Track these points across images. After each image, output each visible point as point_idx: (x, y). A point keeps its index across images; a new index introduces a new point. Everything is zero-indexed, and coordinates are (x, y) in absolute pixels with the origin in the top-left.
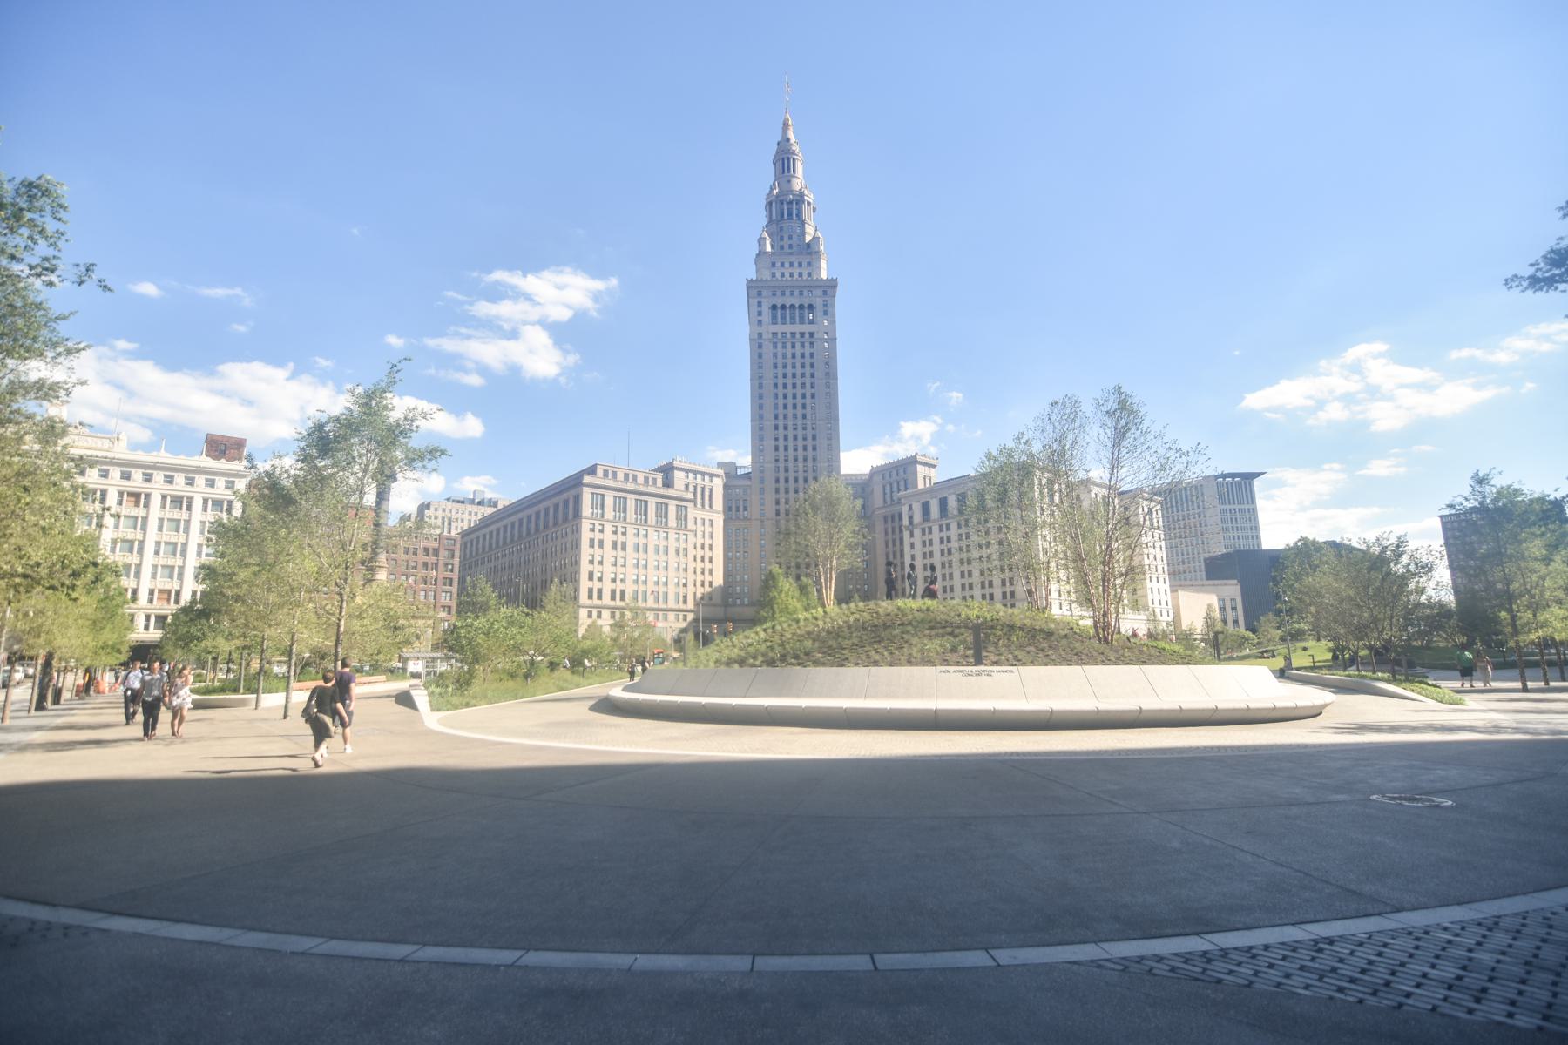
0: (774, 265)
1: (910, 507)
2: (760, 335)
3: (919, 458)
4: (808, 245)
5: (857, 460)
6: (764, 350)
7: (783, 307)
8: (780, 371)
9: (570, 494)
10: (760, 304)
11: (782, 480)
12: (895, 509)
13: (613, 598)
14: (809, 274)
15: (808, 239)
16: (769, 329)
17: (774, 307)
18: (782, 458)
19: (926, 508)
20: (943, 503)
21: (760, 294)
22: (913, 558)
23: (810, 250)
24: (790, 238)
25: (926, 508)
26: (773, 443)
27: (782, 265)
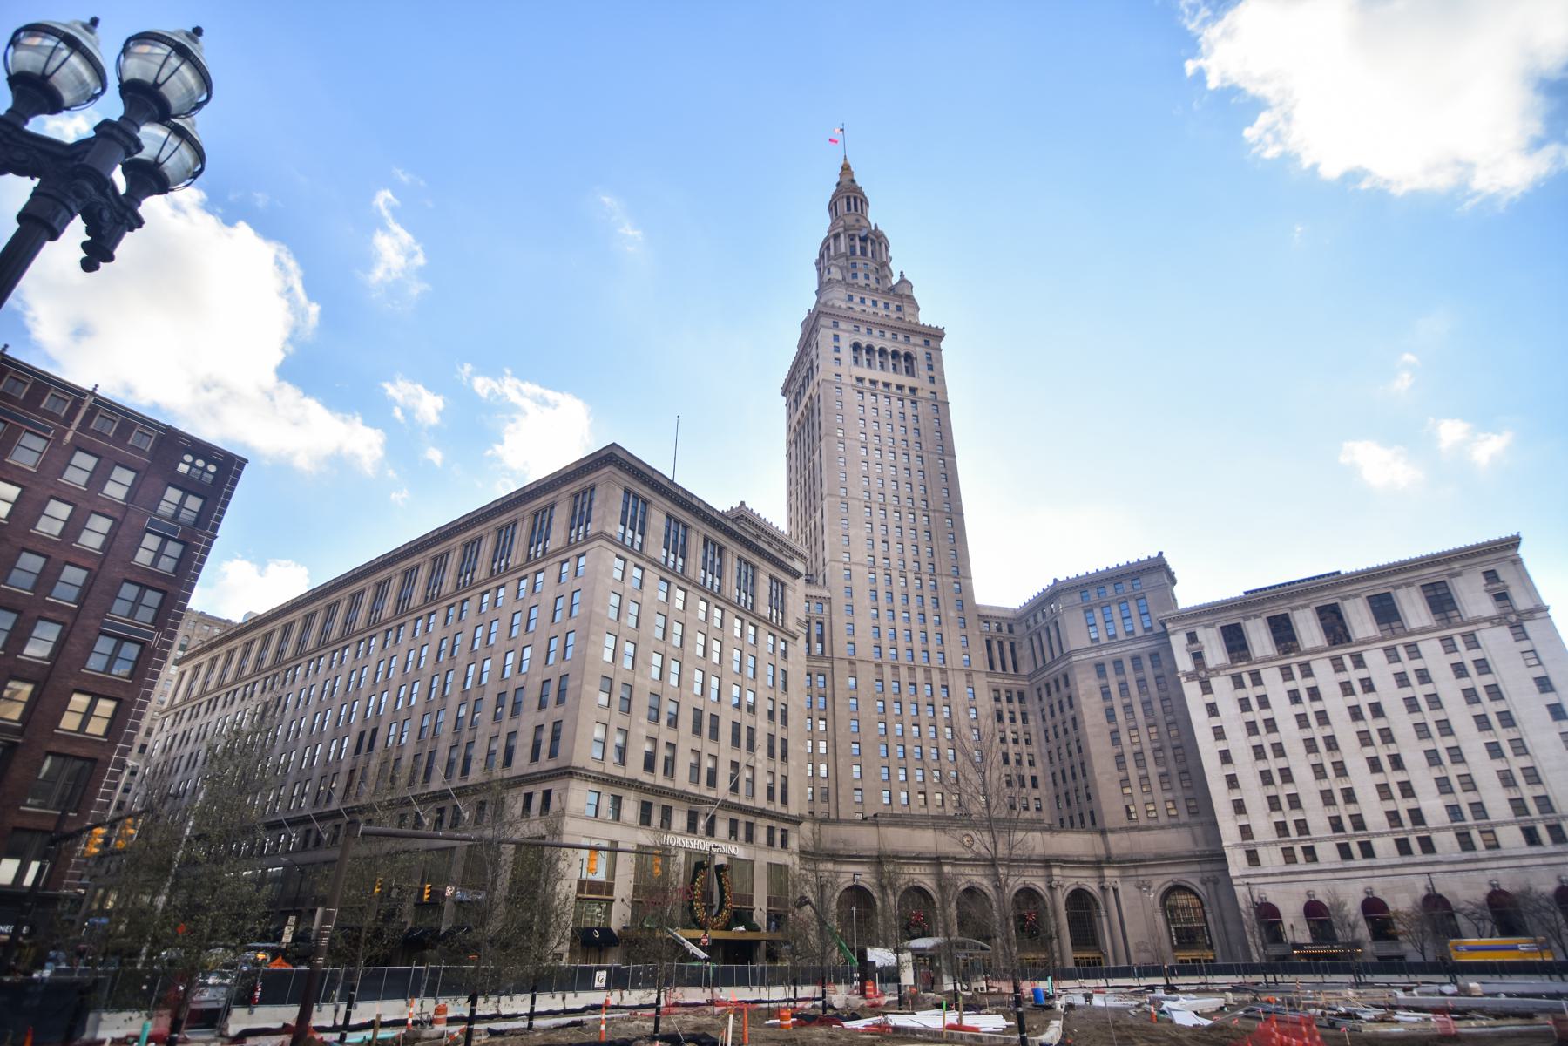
1: (1192, 638)
4: (892, 289)
5: (1004, 577)
6: (845, 398)
7: (870, 349)
9: (575, 487)
10: (836, 338)
11: (882, 595)
13: (649, 765)
16: (850, 370)
17: (856, 347)
18: (881, 561)
19: (1235, 640)
20: (1283, 632)
21: (836, 324)
22: (1219, 733)
25: (1235, 640)
26: (864, 534)
27: (863, 301)
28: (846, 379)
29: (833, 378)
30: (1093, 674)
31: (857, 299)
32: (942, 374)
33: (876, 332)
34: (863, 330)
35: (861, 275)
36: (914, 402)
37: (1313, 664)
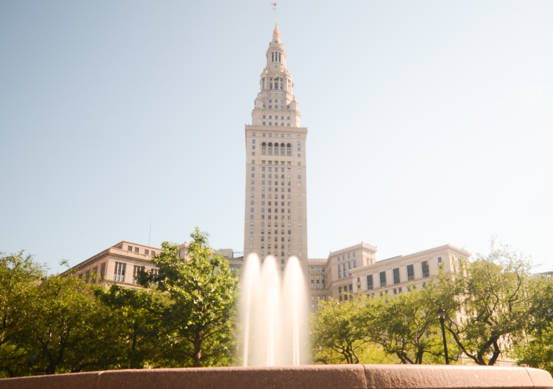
0: (264, 117)
1: (359, 280)
2: (253, 162)
3: (364, 246)
6: (255, 172)
7: (270, 144)
8: (267, 186)
10: (254, 142)
12: (346, 282)
14: (289, 125)
15: (288, 102)
16: (259, 158)
17: (264, 144)
23: (290, 109)
24: (276, 101)
26: (261, 235)
27: (270, 117)
28: (256, 163)
29: (250, 162)
30: (338, 291)
31: (267, 117)
32: (304, 152)
33: (273, 135)
34: (267, 135)
35: (273, 101)
36: (289, 169)
37: (389, 291)
